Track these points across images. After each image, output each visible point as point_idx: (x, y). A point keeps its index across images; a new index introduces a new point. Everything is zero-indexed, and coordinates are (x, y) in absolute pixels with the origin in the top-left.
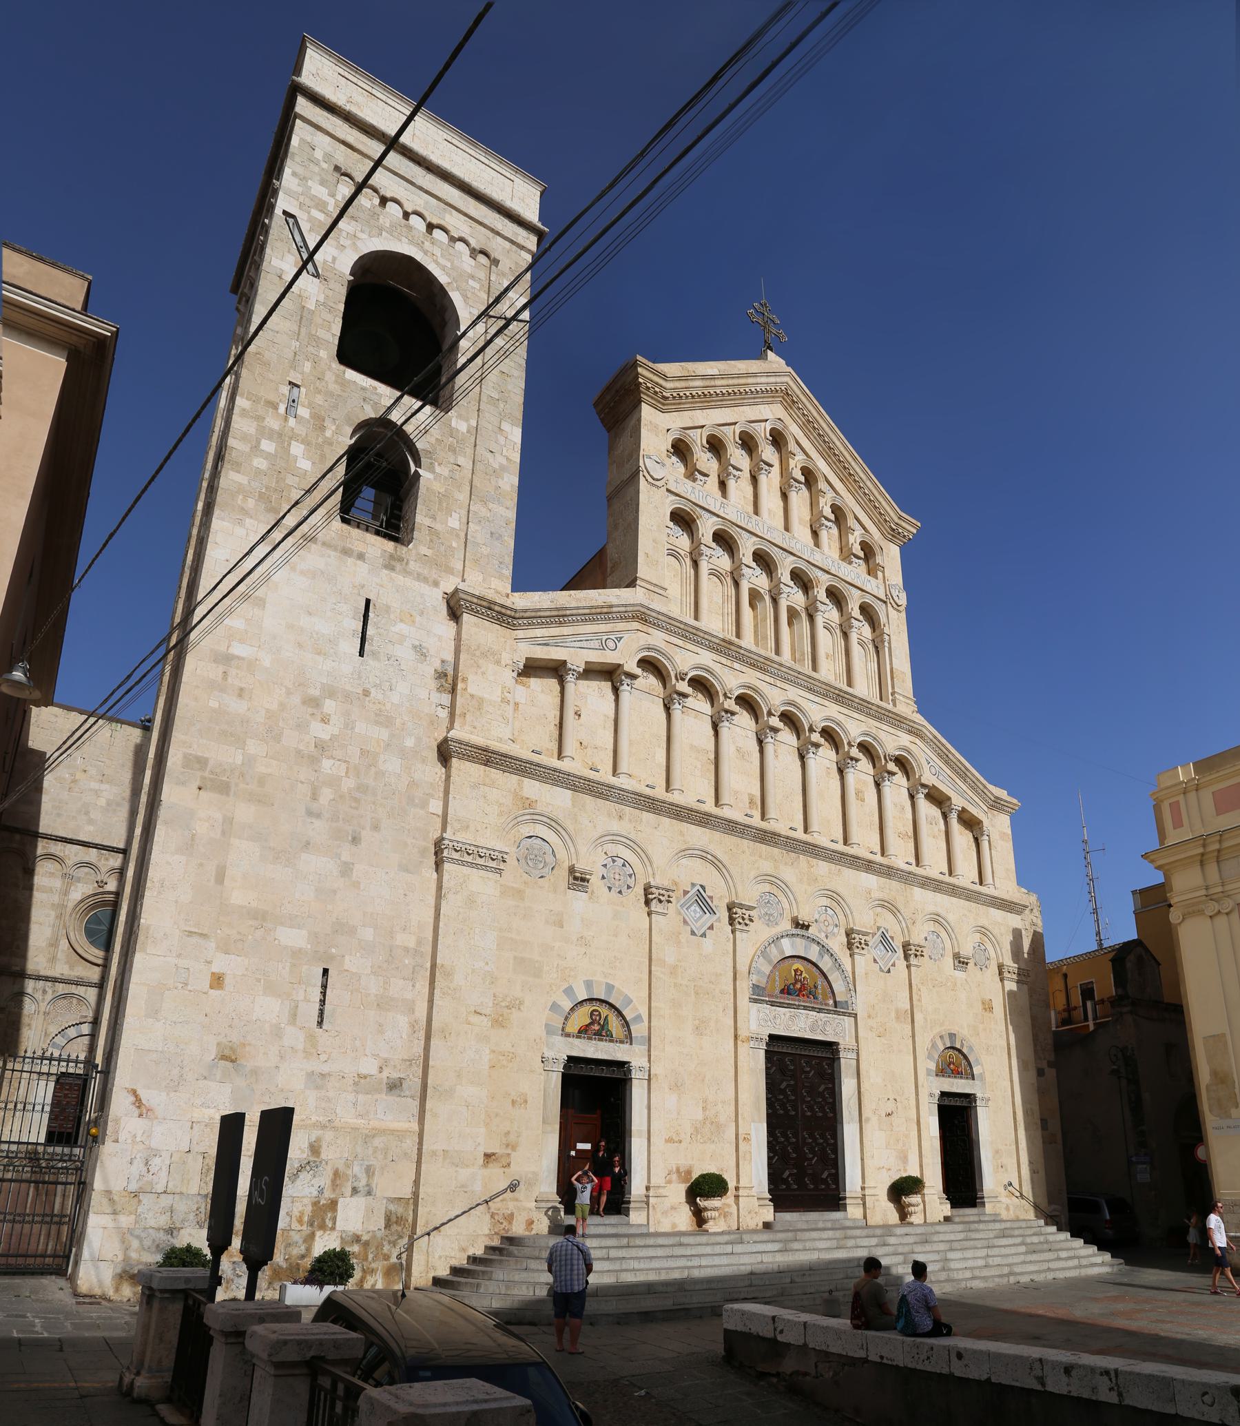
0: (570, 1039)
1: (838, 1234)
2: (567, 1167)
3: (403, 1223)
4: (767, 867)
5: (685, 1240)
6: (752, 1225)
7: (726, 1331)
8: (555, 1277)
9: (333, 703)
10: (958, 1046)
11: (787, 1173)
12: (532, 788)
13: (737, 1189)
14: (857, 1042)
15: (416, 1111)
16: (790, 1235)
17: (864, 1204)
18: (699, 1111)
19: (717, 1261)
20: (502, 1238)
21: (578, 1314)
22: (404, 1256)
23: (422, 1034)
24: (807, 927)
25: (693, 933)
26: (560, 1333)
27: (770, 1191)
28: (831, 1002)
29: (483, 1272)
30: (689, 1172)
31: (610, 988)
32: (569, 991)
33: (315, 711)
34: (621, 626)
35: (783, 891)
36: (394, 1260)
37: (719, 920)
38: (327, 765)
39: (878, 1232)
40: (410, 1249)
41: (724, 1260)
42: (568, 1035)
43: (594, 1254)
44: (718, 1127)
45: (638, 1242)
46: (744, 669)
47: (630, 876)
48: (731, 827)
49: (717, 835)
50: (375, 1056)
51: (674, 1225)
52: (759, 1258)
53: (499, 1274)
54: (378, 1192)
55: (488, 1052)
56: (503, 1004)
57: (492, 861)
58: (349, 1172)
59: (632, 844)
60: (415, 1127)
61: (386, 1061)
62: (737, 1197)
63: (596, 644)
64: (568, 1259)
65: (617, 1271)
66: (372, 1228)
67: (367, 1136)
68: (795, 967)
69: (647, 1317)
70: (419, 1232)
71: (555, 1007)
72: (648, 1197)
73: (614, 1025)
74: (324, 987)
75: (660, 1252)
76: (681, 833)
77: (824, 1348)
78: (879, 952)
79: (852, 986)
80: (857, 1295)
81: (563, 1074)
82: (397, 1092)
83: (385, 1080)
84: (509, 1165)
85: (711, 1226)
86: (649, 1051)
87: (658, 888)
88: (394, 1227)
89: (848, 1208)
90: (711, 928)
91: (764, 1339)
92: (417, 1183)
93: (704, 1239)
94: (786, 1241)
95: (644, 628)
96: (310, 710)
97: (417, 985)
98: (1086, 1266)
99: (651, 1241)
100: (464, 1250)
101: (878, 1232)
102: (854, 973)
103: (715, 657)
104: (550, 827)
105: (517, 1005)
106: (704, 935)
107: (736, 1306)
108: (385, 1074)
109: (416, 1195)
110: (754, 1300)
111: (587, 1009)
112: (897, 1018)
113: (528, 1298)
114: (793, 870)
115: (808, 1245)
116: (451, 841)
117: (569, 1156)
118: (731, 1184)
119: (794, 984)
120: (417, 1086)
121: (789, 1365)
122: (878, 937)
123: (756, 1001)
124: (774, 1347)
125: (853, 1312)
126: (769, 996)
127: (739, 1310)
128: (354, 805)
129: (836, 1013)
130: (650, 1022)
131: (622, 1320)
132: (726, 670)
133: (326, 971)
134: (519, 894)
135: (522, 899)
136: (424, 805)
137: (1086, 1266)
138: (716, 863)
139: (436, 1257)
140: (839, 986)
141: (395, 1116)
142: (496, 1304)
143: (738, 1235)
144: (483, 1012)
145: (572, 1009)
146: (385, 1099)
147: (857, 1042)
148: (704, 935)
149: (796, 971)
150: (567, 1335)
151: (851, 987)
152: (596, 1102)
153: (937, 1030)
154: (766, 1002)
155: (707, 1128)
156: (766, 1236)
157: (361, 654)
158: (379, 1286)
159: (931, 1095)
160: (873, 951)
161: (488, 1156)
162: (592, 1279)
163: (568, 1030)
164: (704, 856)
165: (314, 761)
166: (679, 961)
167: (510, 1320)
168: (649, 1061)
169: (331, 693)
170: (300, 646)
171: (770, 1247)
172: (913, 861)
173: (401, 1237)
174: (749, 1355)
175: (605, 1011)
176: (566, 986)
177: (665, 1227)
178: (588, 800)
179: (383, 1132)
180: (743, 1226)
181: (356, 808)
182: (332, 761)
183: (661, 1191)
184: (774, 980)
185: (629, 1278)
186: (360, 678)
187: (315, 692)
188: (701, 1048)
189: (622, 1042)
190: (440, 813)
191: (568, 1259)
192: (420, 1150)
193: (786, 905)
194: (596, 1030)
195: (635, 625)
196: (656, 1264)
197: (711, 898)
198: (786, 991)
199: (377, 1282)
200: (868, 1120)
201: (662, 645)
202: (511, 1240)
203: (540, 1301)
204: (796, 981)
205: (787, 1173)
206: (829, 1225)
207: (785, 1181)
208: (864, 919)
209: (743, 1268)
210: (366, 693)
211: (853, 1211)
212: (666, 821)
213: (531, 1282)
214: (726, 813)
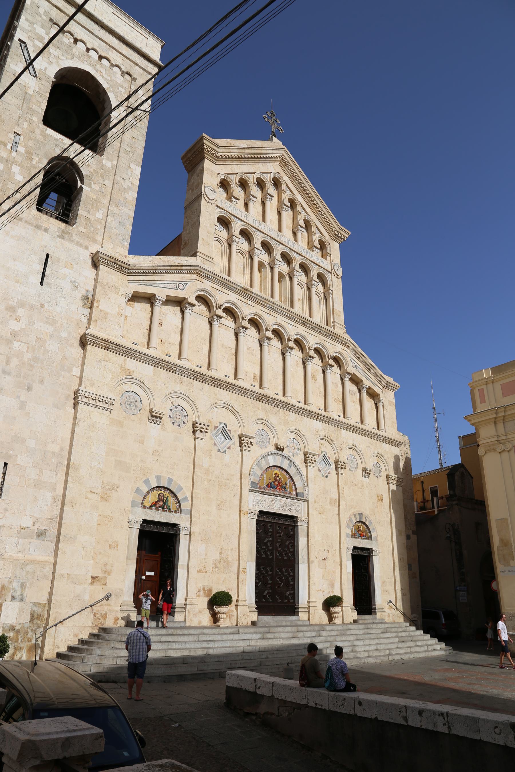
0: (146, 510)
1: (294, 629)
2: (140, 586)
3: (41, 619)
4: (261, 414)
5: (206, 631)
6: (245, 623)
7: (227, 687)
8: (130, 653)
9: (23, 310)
10: (364, 521)
11: (266, 592)
12: (131, 364)
13: (237, 601)
14: (308, 516)
15: (53, 550)
16: (266, 629)
17: (309, 612)
18: (217, 557)
19: (224, 644)
20: (100, 628)
21: (141, 676)
22: (40, 639)
23: (59, 504)
24: (283, 450)
25: (219, 451)
26: (131, 687)
27: (256, 603)
28: (294, 493)
29: (87, 650)
30: (210, 591)
31: (170, 480)
32: (147, 482)
33: (12, 314)
34: (187, 277)
35: (270, 429)
36: (34, 641)
37: (234, 444)
38: (16, 345)
39: (316, 628)
40: (44, 635)
41: (228, 644)
42: (145, 507)
43: (153, 639)
44: (228, 564)
45: (179, 632)
46: (254, 304)
47: (185, 416)
48: (243, 391)
50: (32, 516)
51: (200, 622)
52: (248, 643)
53: (96, 651)
54: (27, 599)
55: (97, 515)
56: (107, 487)
57: (105, 404)
58: (11, 587)
59: (187, 399)
60: (52, 559)
61: (37, 519)
62: (237, 606)
63: (173, 286)
64: (138, 643)
65: (165, 650)
66: (22, 621)
67: (23, 564)
68: (275, 472)
69: (182, 678)
70: (50, 624)
71: (138, 491)
72: (185, 605)
73: (172, 502)
74: (4, 473)
75: (191, 638)
76: (215, 394)
77: (283, 698)
78: (322, 465)
79: (306, 485)
80: (303, 666)
81: (140, 530)
82: (42, 538)
83: (36, 531)
84: (106, 584)
85: (221, 623)
86: (191, 518)
87: (200, 424)
88: (36, 621)
89: (300, 614)
90: (229, 448)
91: (249, 692)
92: (51, 594)
93: (217, 631)
94: (264, 633)
95: (200, 279)
96: (9, 314)
97: (59, 474)
98: (431, 651)
99: (186, 632)
100: (76, 635)
101: (316, 628)
102: (307, 477)
103: (238, 297)
104: (140, 386)
105: (115, 488)
106: (225, 452)
107: (234, 672)
108: (36, 527)
109: (50, 601)
110: (244, 668)
111: (157, 492)
112: (331, 503)
113: (113, 666)
114: (277, 417)
115: (277, 635)
116: (84, 391)
117: (141, 579)
118: (234, 598)
119: (274, 482)
120: (54, 534)
121: (263, 708)
122: (321, 457)
123: (252, 491)
124: (255, 698)
125: (300, 677)
126: (260, 488)
127: (235, 675)
128: (30, 368)
129: (297, 499)
130: (192, 501)
131: (167, 679)
132: (244, 304)
133: (6, 464)
134: (120, 424)
135: (122, 427)
136: (70, 370)
137: (431, 651)
138: (234, 412)
139: (59, 640)
140: (299, 484)
141: (40, 552)
142: (94, 669)
143: (237, 628)
144: (95, 492)
145: (148, 492)
146: (36, 542)
147: (308, 516)
148: (225, 452)
149: (275, 474)
150: (134, 689)
151: (306, 485)
152: (158, 546)
153: (352, 511)
154: (258, 492)
155: (221, 565)
156: (252, 630)
157: (41, 284)
158: (24, 658)
159: (348, 548)
160: (318, 464)
161: (93, 578)
162: (151, 654)
163: (145, 504)
164: (228, 407)
165: (9, 342)
167: (100, 680)
168: (191, 524)
169: (22, 305)
170: (7, 277)
171: (255, 636)
172: (342, 415)
173: (39, 627)
174: (240, 703)
175: (166, 494)
176: (145, 478)
177: (195, 624)
178: (163, 373)
179: (32, 562)
180: (240, 623)
181: (31, 371)
182: (20, 343)
183: (194, 602)
184: (263, 480)
185: (172, 654)
186: (39, 297)
187: (13, 303)
188: (221, 517)
189: (175, 512)
190: (79, 376)
191: (138, 643)
192: (54, 573)
193: (271, 437)
194: (161, 505)
195: (195, 277)
196: (188, 646)
197: (230, 431)
198: (270, 486)
199: (23, 655)
200: (313, 562)
201: (209, 289)
202: (104, 630)
203: (121, 668)
204: (276, 480)
205: (266, 592)
206: (289, 624)
207: (265, 597)
208: (314, 446)
209: (238, 649)
210: (42, 306)
211: (303, 616)
212: (207, 386)
213: (115, 656)
214: (240, 383)
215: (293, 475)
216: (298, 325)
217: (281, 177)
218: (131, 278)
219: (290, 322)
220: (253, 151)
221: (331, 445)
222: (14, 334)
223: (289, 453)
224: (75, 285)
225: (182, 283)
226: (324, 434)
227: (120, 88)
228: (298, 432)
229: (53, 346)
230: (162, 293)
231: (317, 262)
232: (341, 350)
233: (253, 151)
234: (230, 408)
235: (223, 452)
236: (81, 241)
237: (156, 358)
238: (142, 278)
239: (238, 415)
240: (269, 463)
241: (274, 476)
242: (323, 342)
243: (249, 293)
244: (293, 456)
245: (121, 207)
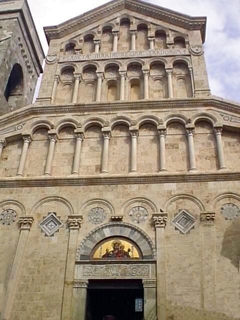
4: (94, 195)
25: (46, 235)
35: (107, 205)
46: (90, 113)
49: (64, 188)
59: (17, 203)
76: (43, 192)
90: (58, 231)
103: (74, 114)
138: (64, 201)
148: (53, 235)
164: (56, 199)
166: (36, 249)
195: (32, 116)
197: (59, 217)
215: (137, 240)
216: (143, 111)
217: (128, 15)
219: (133, 111)
220: (91, 14)
221: (193, 200)
223: (133, 220)
225: (21, 125)
226: (180, 192)
228: (144, 199)
231: (171, 54)
232: (204, 112)
233: (91, 14)
234: (59, 199)
235: (51, 236)
239: (67, 203)
240: (104, 235)
241: (113, 245)
242: (178, 113)
243: (82, 107)
244: (138, 222)
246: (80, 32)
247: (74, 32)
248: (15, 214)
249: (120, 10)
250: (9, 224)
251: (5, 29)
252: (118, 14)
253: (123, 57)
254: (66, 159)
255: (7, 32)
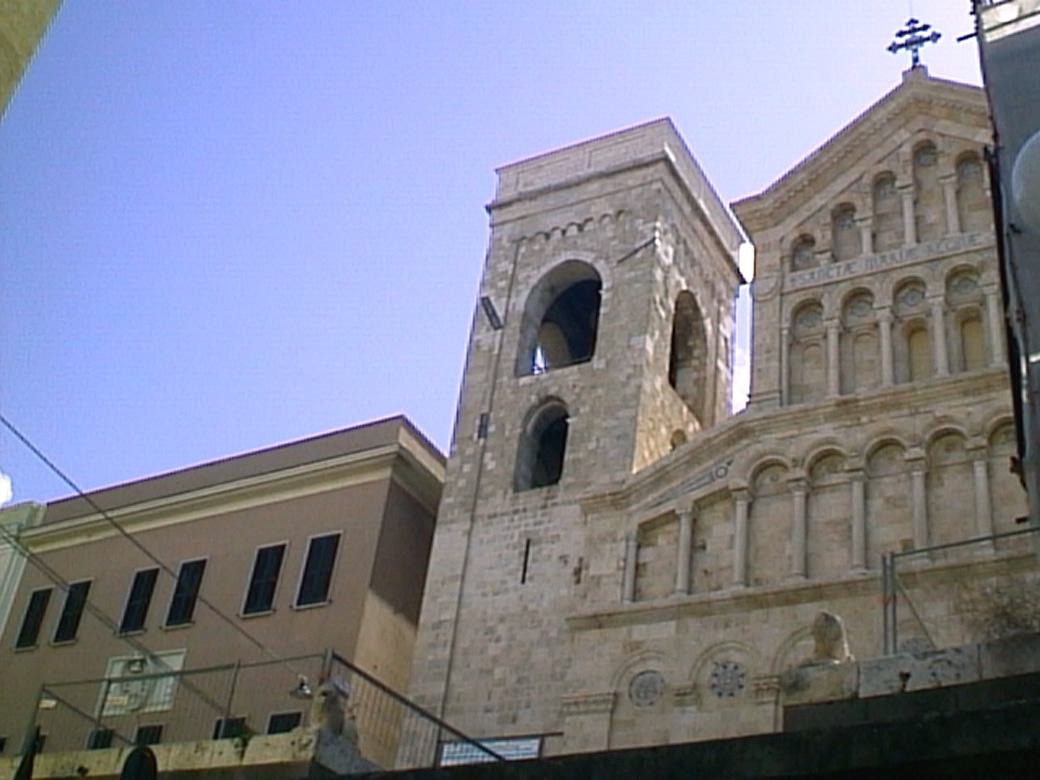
34: (728, 452)
76: (795, 616)
103: (836, 424)
178: (693, 623)
195: (745, 442)
216: (993, 395)
218: (633, 507)
222: (495, 660)
224: (564, 559)
227: (614, 243)
229: (540, 655)
230: (682, 505)
236: (571, 497)
237: (672, 607)
238: (650, 498)
245: (621, 414)
246: (818, 201)
247: (805, 202)
248: (740, 672)
249: (907, 122)
250: (732, 695)
251: (638, 217)
252: (904, 135)
253: (932, 256)
254: (835, 532)
255: (645, 223)
